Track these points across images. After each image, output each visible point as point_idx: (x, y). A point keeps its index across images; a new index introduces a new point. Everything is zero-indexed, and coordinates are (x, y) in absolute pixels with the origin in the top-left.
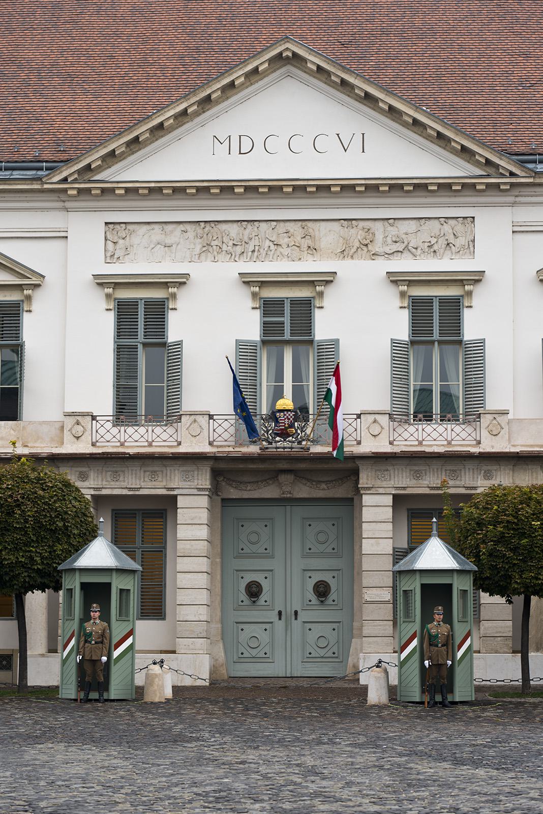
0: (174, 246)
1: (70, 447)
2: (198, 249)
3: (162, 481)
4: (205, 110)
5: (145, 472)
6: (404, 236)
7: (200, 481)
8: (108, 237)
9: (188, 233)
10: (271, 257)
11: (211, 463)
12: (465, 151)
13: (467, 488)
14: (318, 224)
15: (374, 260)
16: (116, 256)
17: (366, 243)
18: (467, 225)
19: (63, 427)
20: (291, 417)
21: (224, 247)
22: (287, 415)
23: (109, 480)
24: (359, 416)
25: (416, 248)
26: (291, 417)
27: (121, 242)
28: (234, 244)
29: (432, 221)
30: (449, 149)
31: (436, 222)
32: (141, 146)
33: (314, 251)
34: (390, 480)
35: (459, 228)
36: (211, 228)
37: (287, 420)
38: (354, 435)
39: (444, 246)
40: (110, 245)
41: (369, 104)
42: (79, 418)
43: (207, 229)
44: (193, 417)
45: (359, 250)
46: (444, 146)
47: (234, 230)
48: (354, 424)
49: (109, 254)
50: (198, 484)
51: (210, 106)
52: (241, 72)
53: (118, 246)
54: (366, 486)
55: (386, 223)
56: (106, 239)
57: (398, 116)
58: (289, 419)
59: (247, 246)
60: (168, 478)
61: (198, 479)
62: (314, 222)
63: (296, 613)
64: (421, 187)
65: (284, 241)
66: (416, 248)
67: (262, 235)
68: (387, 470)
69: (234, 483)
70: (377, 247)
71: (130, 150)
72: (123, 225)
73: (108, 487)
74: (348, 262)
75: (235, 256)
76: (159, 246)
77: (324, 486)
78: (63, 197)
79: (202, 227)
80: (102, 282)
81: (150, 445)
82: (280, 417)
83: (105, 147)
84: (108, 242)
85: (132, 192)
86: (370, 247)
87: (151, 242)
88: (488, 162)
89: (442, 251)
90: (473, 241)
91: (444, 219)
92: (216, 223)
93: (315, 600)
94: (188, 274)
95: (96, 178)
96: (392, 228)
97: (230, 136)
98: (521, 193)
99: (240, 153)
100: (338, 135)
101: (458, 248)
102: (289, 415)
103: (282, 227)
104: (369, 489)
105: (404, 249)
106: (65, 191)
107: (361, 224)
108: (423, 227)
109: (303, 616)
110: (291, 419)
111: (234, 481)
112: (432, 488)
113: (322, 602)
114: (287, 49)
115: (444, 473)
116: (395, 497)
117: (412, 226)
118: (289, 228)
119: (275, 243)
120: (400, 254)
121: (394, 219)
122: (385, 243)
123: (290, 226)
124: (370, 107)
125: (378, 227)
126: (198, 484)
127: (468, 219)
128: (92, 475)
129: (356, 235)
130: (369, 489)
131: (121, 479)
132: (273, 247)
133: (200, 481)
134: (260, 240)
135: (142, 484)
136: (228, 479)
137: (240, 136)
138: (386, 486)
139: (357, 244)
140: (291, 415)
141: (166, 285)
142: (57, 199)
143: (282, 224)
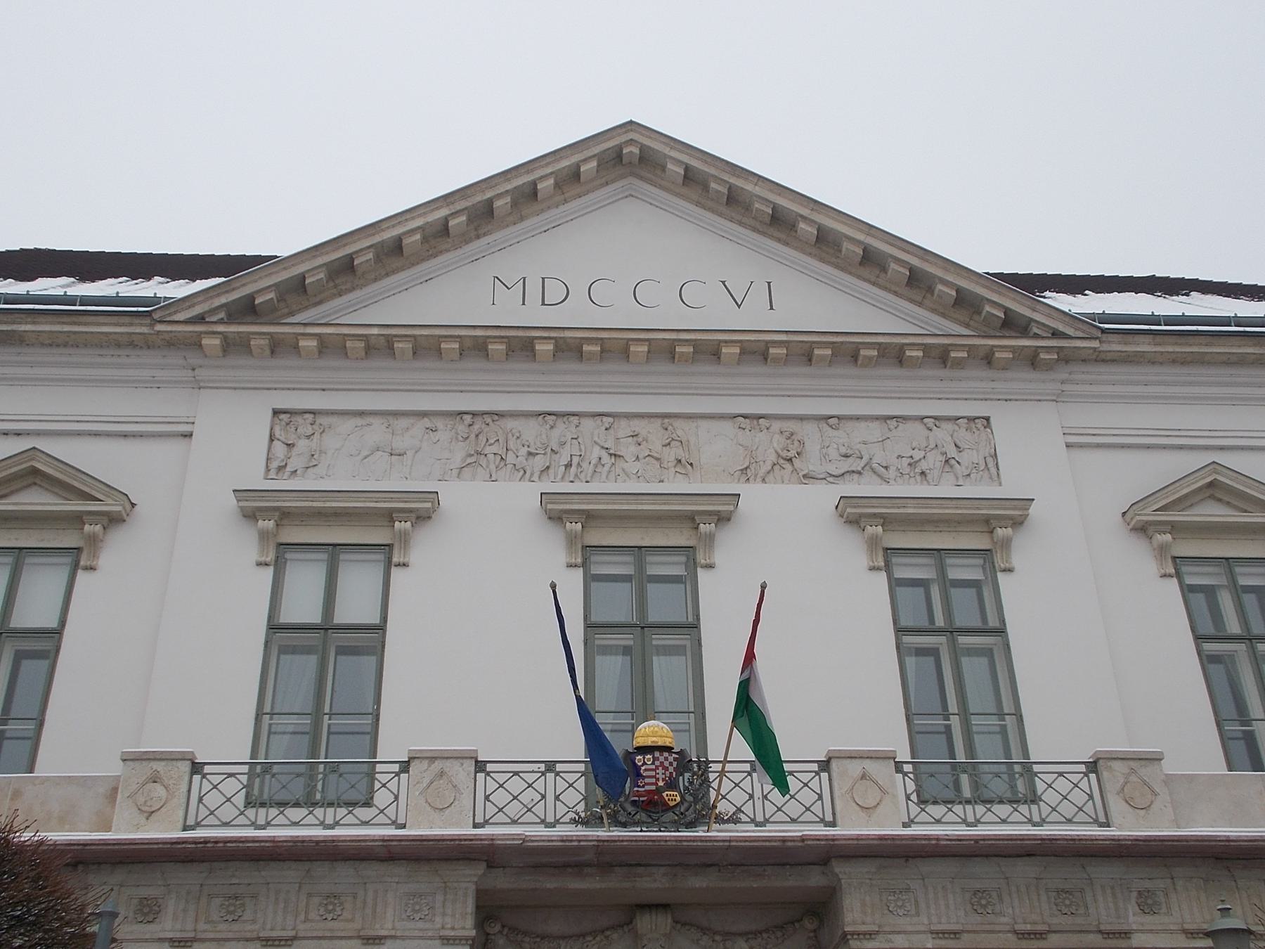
1: (126, 829)
3: (352, 920)
4: (482, 231)
5: (310, 895)
7: (448, 919)
8: (277, 435)
11: (480, 869)
16: (289, 469)
17: (790, 455)
19: (115, 790)
20: (671, 764)
21: (510, 458)
22: (662, 759)
23: (215, 917)
24: (825, 766)
25: (886, 468)
26: (671, 764)
28: (530, 454)
31: (918, 426)
34: (918, 914)
35: (963, 435)
37: (660, 771)
39: (938, 464)
42: (159, 766)
43: (476, 427)
44: (438, 765)
45: (777, 467)
46: (919, 298)
47: (531, 431)
48: (814, 784)
49: (274, 465)
50: (443, 928)
51: (490, 227)
52: (549, 170)
53: (295, 451)
54: (863, 928)
55: (823, 425)
58: (666, 769)
59: (554, 456)
60: (369, 911)
61: (444, 914)
65: (629, 449)
68: (908, 890)
69: (527, 939)
70: (811, 463)
71: (336, 286)
72: (310, 417)
73: (212, 935)
75: (532, 475)
76: (380, 453)
82: (645, 763)
83: (285, 269)
86: (796, 462)
89: (936, 473)
96: (835, 433)
98: (1073, 376)
99: (543, 304)
100: (723, 282)
102: (666, 759)
103: (624, 428)
107: (776, 426)
110: (671, 769)
111: (525, 933)
115: (1044, 898)
117: (874, 431)
118: (637, 429)
120: (856, 476)
121: (839, 417)
122: (825, 457)
123: (638, 425)
124: (779, 240)
125: (809, 432)
126: (443, 928)
128: (171, 905)
129: (768, 444)
131: (248, 915)
132: (606, 459)
133: (448, 919)
135: (301, 927)
136: (513, 929)
138: (910, 928)
139: (773, 458)
140: (671, 759)
141: (389, 517)
142: (181, 362)
143: (624, 422)
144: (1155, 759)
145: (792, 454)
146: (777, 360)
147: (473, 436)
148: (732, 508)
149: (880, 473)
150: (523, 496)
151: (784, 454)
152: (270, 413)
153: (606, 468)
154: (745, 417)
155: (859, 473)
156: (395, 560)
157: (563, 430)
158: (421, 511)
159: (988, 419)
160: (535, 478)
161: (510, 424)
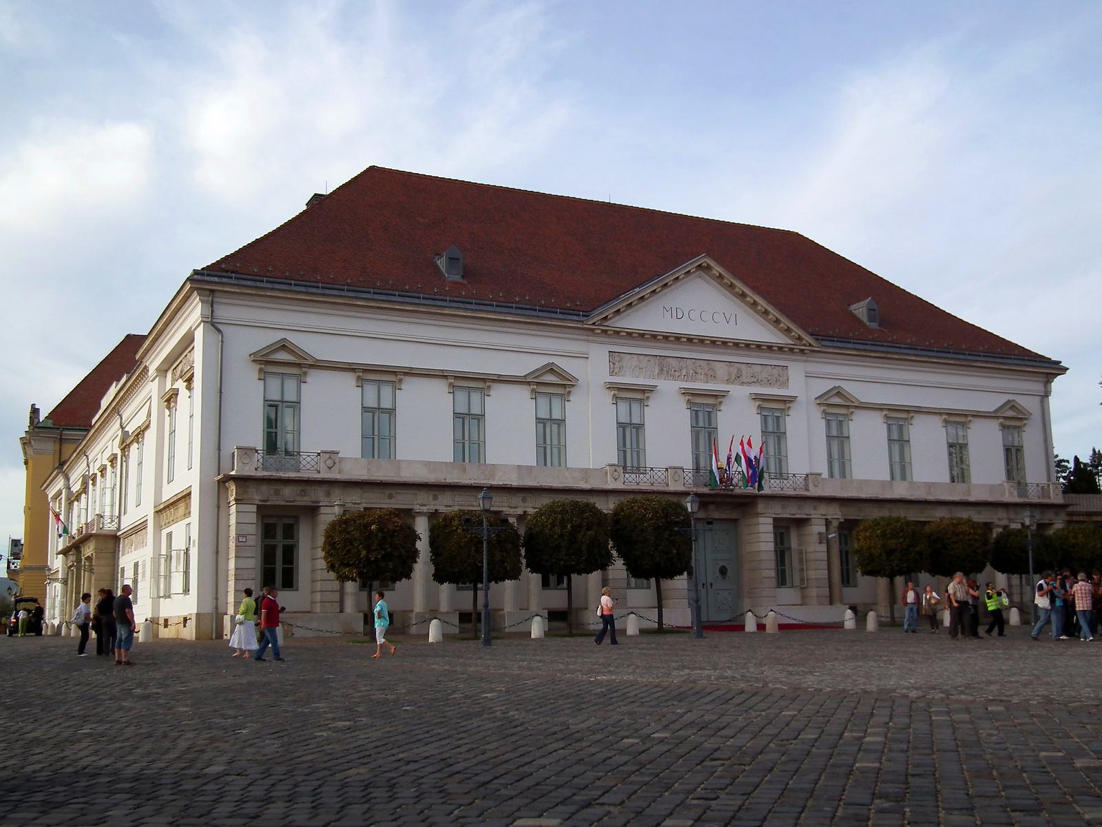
2: (657, 371)
12: (788, 330)
13: (807, 515)
14: (715, 362)
38: (315, 467)
47: (674, 362)
63: (711, 584)
64: (770, 348)
70: (744, 379)
77: (728, 512)
78: (589, 333)
80: (611, 387)
81: (652, 485)
88: (800, 338)
90: (788, 380)
93: (720, 576)
95: (605, 324)
104: (762, 514)
106: (593, 330)
107: (736, 365)
109: (714, 587)
112: (287, 502)
113: (724, 578)
114: (705, 262)
116: (775, 519)
122: (747, 377)
130: (762, 514)
132: (694, 374)
144: (820, 475)
161: (669, 359)
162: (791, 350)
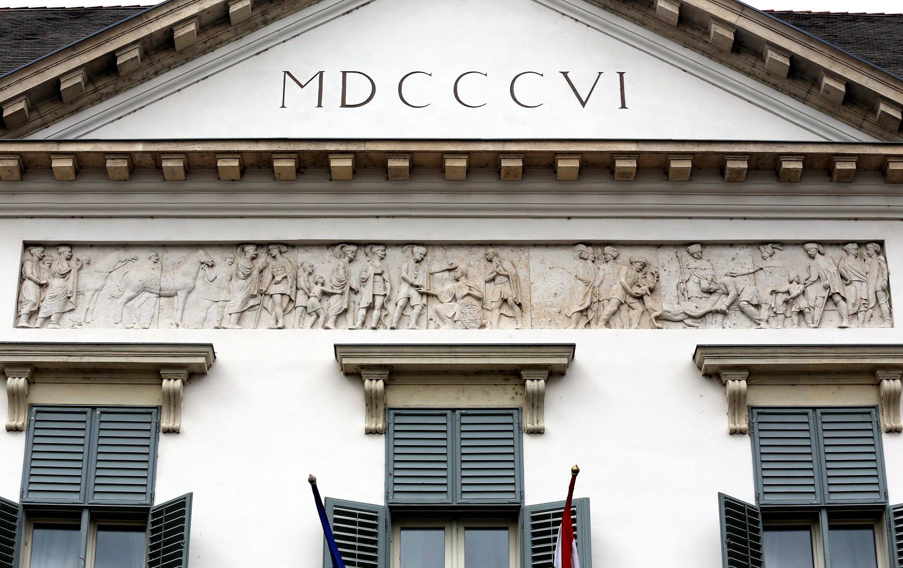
0: (182, 295)
2: (237, 301)
4: (269, 17)
6: (727, 280)
8: (28, 271)
9: (215, 268)
10: (414, 322)
15: (659, 328)
16: (42, 314)
17: (639, 291)
18: (869, 260)
21: (301, 299)
25: (758, 306)
27: (56, 283)
28: (325, 294)
29: (789, 252)
30: (817, 101)
32: (120, 84)
33: (517, 309)
35: (851, 264)
36: (269, 259)
39: (821, 302)
40: (30, 290)
41: (632, 13)
45: (624, 308)
47: (327, 266)
49: (25, 310)
51: (280, 10)
53: (49, 293)
55: (682, 252)
56: (22, 278)
57: (697, 34)
62: (515, 249)
65: (444, 286)
66: (758, 306)
67: (393, 275)
70: (667, 303)
71: (96, 90)
72: (65, 251)
74: (598, 333)
76: (147, 294)
79: (249, 255)
84: (27, 283)
85: (89, 167)
87: (127, 285)
89: (817, 313)
90: (887, 290)
91: (815, 246)
92: (284, 249)
94: (211, 346)
96: (698, 264)
97: (321, 73)
99: (344, 105)
100: (565, 74)
101: (854, 305)
103: (438, 260)
105: (728, 308)
107: (626, 254)
108: (770, 262)
117: (746, 259)
118: (456, 262)
119: (423, 290)
120: (719, 317)
122: (683, 293)
123: (457, 257)
127: (869, 246)
129: (615, 277)
132: (416, 299)
134: (388, 285)
137: (344, 73)
139: (617, 294)
143: (439, 253)
145: (644, 289)
146: (625, 175)
147: (256, 272)
148: (564, 361)
149: (750, 311)
150: (312, 347)
151: (636, 290)
152: (20, 246)
153: (417, 310)
154: (587, 244)
155: (724, 313)
156: (164, 424)
157: (366, 265)
158: (194, 368)
159: (881, 243)
160: (330, 324)
161: (302, 257)
162: (875, 170)
